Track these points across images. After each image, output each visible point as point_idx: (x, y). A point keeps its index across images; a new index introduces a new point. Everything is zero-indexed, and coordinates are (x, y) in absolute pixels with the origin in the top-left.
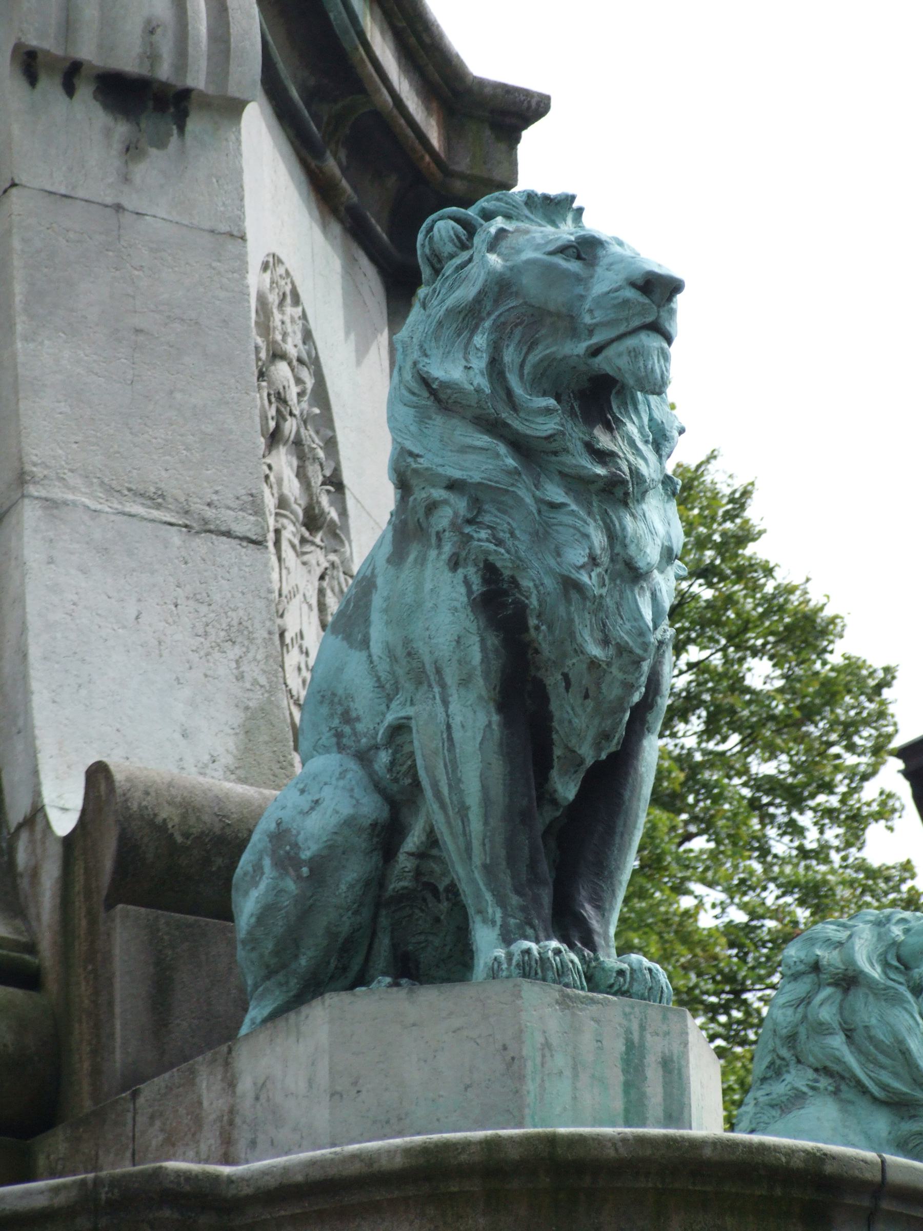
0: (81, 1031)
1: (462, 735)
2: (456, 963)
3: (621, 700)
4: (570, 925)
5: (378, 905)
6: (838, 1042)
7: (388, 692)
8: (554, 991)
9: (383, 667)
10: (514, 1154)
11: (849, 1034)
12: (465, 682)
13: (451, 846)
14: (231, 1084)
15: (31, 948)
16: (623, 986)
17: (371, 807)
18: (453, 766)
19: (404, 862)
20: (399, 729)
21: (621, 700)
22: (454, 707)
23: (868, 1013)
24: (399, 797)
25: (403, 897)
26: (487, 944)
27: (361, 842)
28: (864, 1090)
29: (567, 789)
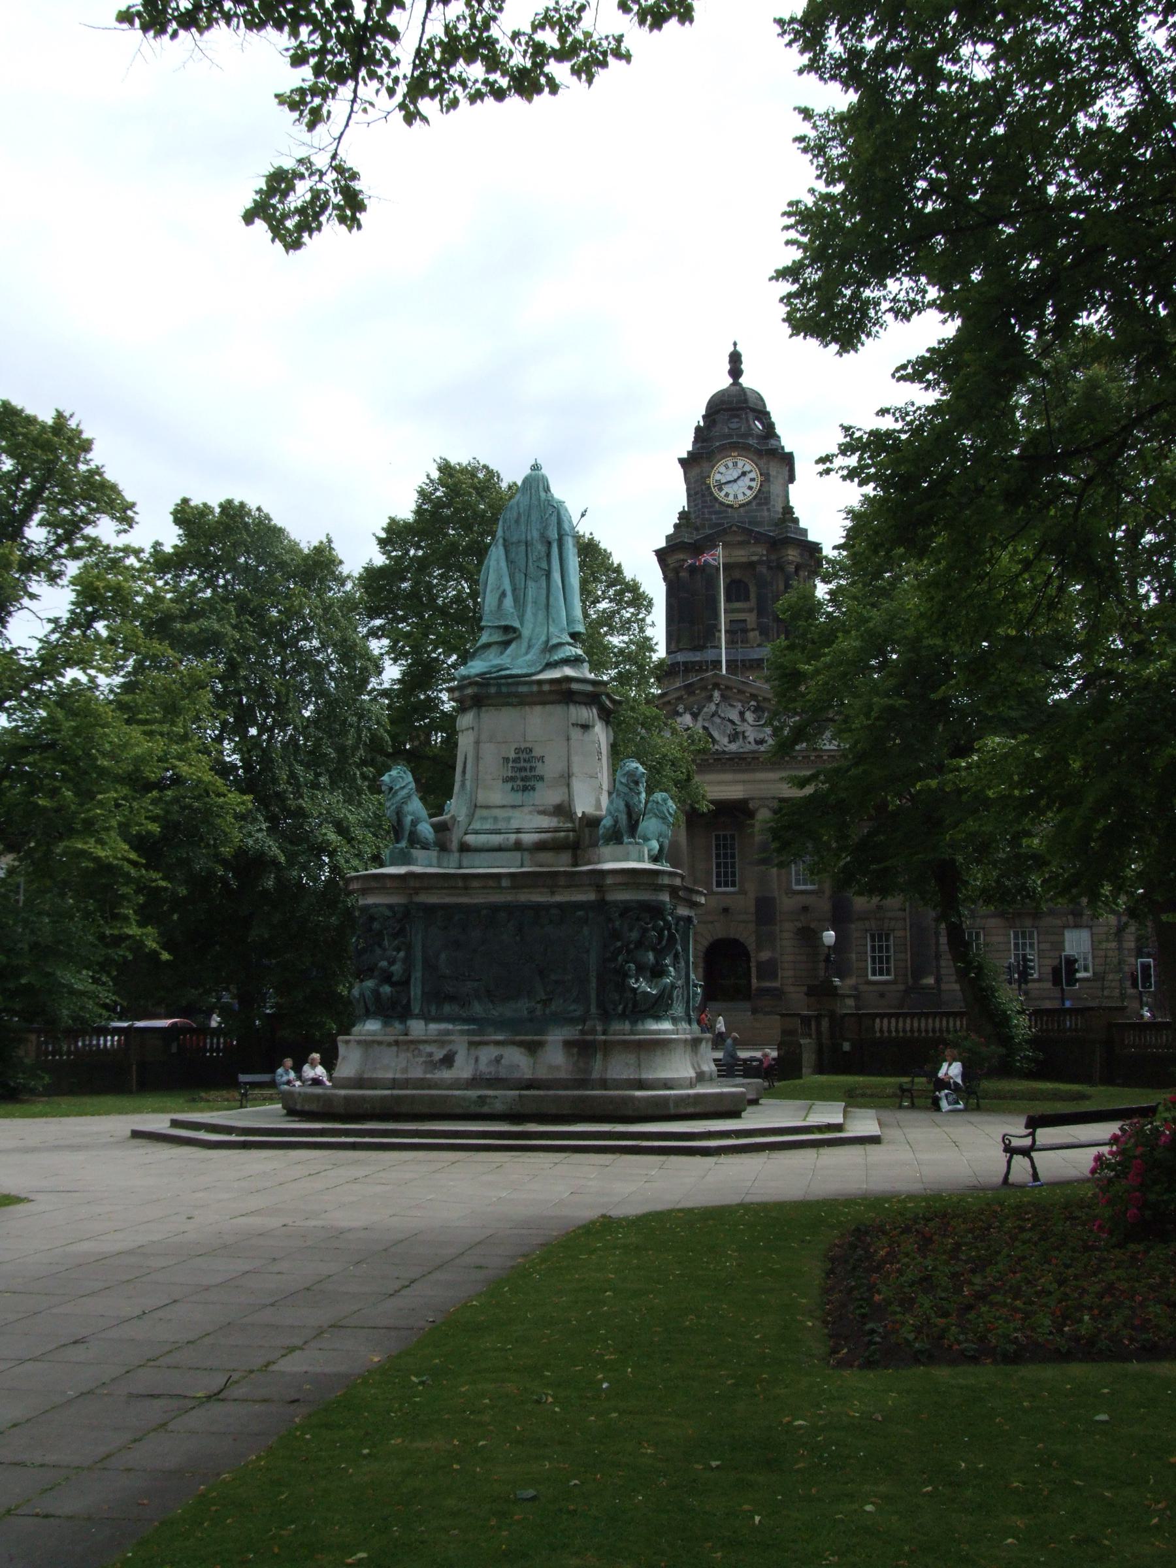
1: (623, 818)
2: (622, 843)
4: (634, 837)
24: (616, 822)
26: (626, 840)
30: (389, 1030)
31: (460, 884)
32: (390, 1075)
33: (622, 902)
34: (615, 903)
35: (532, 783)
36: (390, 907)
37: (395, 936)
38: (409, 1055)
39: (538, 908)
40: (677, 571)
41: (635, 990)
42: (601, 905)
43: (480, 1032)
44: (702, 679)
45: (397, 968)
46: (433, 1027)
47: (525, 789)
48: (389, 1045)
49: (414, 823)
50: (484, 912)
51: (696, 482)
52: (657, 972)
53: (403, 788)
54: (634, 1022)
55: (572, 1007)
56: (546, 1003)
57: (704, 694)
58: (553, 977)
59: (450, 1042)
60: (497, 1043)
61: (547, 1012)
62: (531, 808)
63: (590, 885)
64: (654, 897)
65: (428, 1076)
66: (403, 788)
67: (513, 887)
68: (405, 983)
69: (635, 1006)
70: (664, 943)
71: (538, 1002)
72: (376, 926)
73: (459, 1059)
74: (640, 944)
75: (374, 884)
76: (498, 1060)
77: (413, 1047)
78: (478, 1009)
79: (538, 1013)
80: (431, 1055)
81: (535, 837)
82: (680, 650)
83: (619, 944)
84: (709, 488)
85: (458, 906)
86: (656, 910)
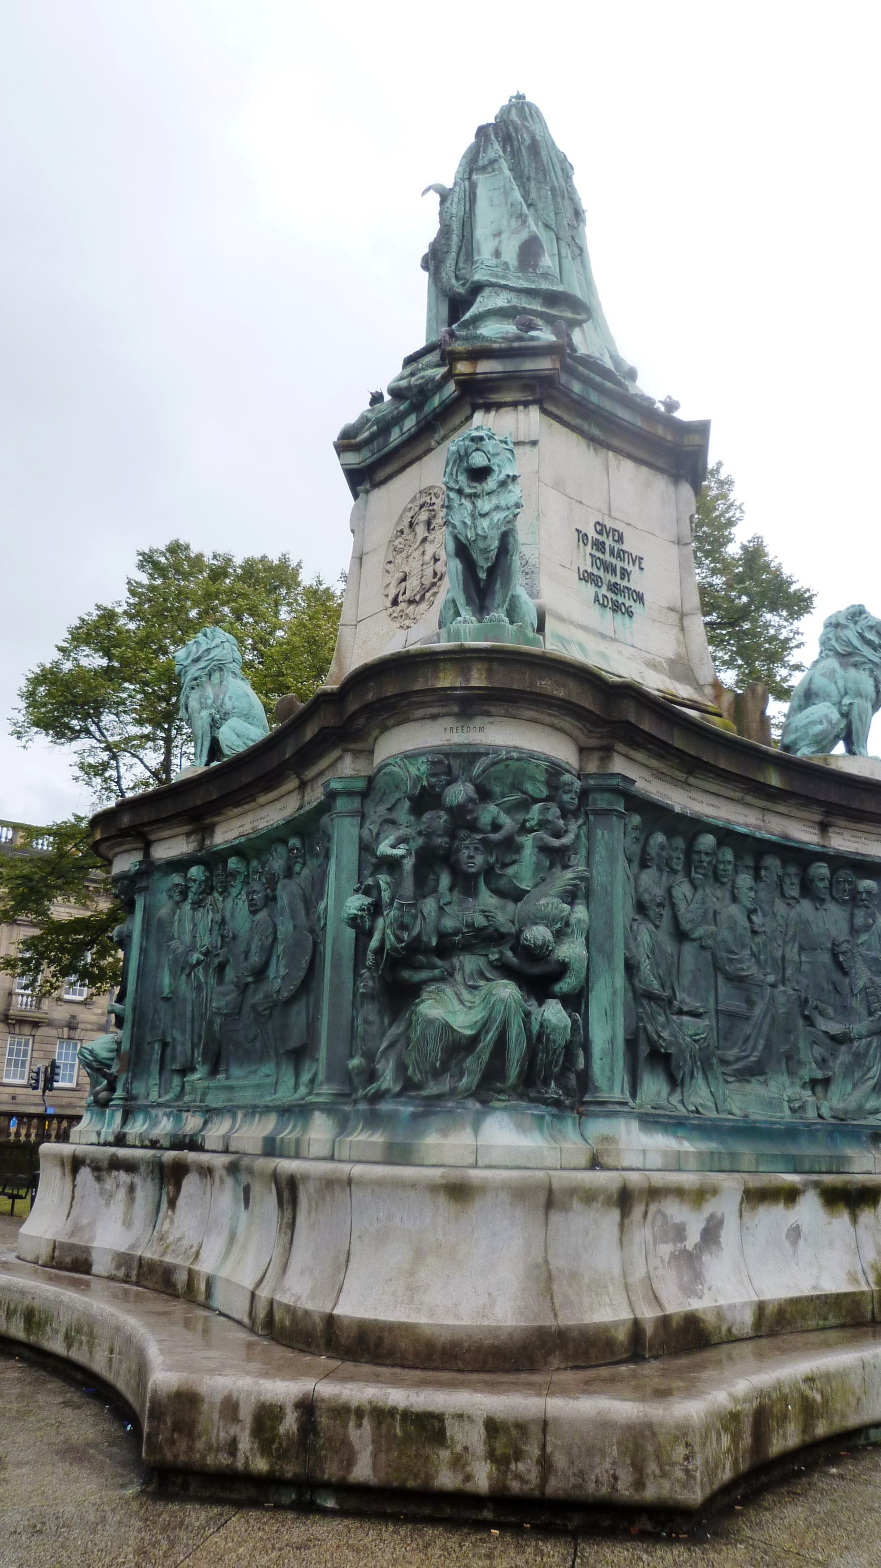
47: (616, 608)
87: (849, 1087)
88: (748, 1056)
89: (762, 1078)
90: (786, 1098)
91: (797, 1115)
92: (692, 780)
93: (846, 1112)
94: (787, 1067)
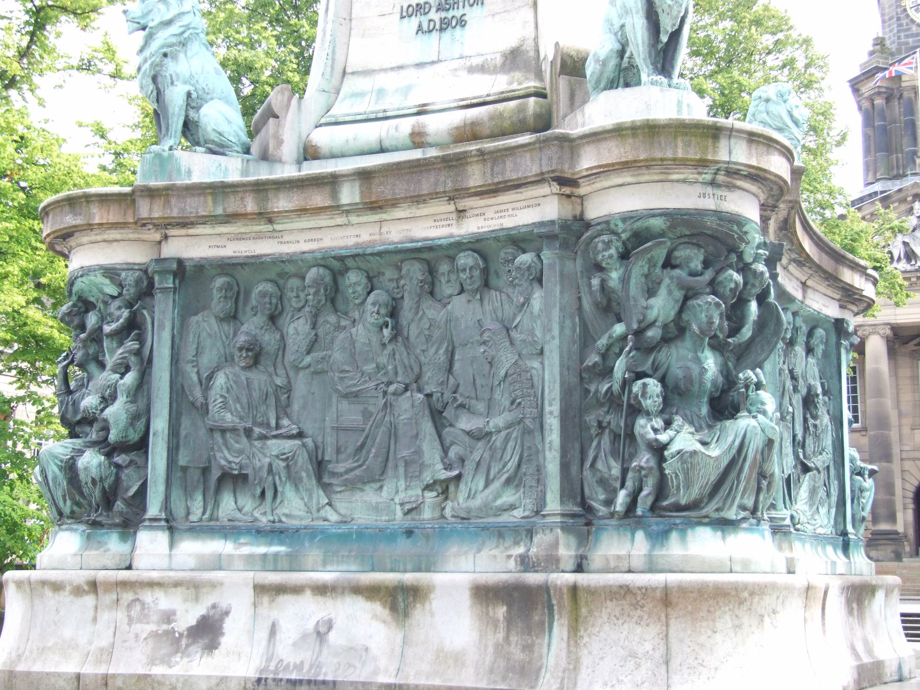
0: (555, 107)
3: (677, 16)
5: (620, 71)
6: (764, 115)
7: (620, 17)
8: (658, 88)
9: (619, 11)
10: (639, 124)
11: (768, 113)
12: (637, 12)
13: (635, 55)
14: (584, 116)
15: (545, 89)
16: (677, 87)
17: (617, 46)
18: (635, 34)
19: (626, 60)
20: (623, 26)
21: (677, 16)
22: (635, 19)
23: (772, 107)
25: (626, 69)
27: (615, 55)
28: (771, 126)
29: (664, 38)
30: (94, 556)
31: (250, 206)
32: (70, 667)
33: (627, 218)
34: (606, 225)
35: (458, 13)
36: (111, 272)
37: (121, 335)
38: (121, 615)
39: (430, 258)
40: (871, 100)
41: (659, 450)
42: (573, 233)
43: (293, 563)
44: (900, 190)
45: (117, 412)
46: (192, 549)
47: (445, 25)
48: (78, 591)
49: (192, 102)
50: (312, 273)
51: (890, 6)
52: (725, 404)
53: (169, 23)
54: (659, 537)
55: (508, 497)
56: (444, 488)
57: (904, 207)
58: (465, 423)
59: (214, 585)
60: (322, 590)
61: (448, 512)
62: (456, 64)
63: (540, 180)
64: (709, 204)
65: (158, 670)
66: (169, 23)
67: (374, 206)
68: (142, 445)
69: (661, 490)
70: (747, 332)
71: (428, 487)
72: (92, 320)
73: (233, 631)
74: (676, 330)
75: (69, 220)
76: (321, 633)
77: (128, 596)
78: (294, 506)
79: (427, 514)
80: (168, 617)
81: (458, 117)
82: (878, 180)
83: (619, 329)
84: (905, 10)
85: (255, 264)
86: (717, 240)
87: (481, 484)
88: (361, 466)
89: (376, 485)
90: (397, 500)
91: (409, 517)
92: (278, 227)
93: (469, 511)
94: (406, 471)
